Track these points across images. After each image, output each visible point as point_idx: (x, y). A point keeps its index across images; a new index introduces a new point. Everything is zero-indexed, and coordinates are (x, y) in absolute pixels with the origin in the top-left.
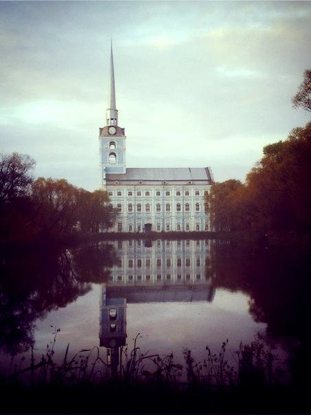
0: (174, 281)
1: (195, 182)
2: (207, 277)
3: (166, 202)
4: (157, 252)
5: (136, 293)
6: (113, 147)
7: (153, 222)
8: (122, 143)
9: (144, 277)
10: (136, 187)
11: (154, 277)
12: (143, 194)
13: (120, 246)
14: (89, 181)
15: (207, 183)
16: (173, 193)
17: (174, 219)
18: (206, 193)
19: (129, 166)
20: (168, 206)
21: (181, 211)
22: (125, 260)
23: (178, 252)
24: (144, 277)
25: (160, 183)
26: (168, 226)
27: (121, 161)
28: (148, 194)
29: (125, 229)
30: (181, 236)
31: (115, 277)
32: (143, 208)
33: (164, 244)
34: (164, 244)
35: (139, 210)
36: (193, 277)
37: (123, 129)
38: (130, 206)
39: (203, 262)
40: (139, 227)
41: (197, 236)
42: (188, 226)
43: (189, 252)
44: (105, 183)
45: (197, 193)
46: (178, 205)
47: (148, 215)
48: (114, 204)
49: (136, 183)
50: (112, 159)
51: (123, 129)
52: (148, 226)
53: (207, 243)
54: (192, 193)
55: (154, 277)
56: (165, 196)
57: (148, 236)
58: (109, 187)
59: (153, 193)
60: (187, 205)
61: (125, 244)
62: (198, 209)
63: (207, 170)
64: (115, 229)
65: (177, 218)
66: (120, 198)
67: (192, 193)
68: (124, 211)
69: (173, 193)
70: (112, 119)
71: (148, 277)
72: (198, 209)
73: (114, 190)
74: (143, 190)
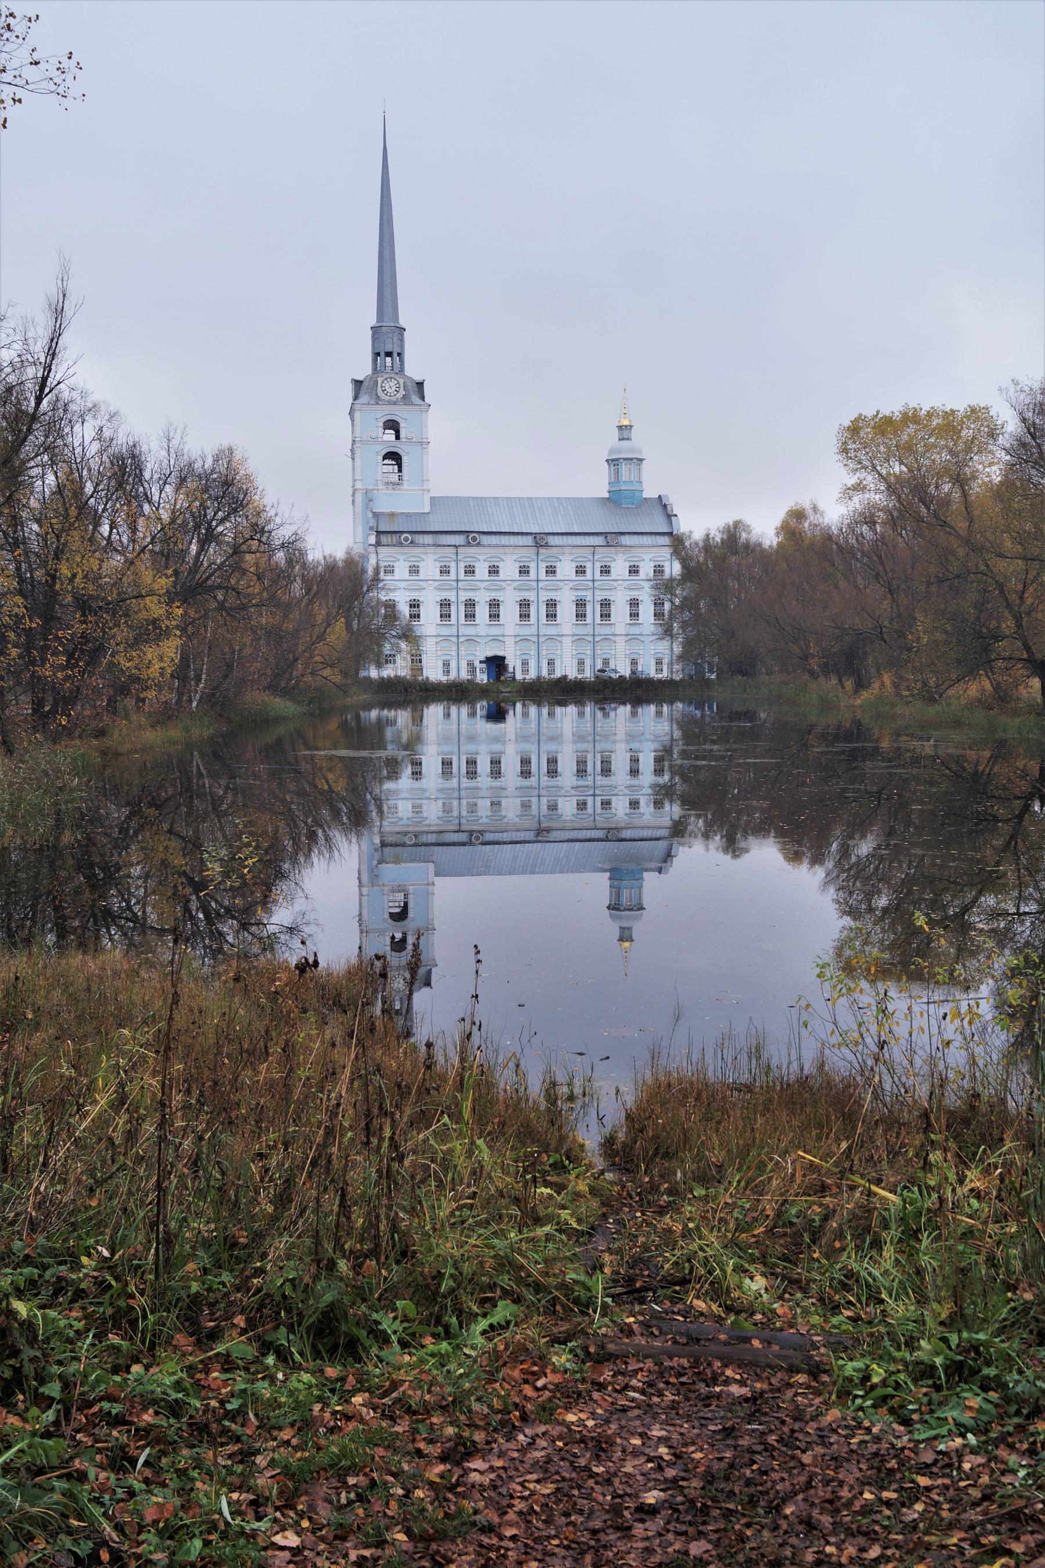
2: (658, 804)
4: (522, 738)
5: (464, 842)
6: (390, 436)
10: (460, 550)
12: (482, 571)
13: (418, 719)
14: (328, 536)
16: (566, 569)
17: (567, 642)
18: (659, 570)
19: (438, 490)
20: (552, 604)
21: (589, 619)
22: (431, 759)
23: (579, 738)
24: (484, 805)
25: (529, 540)
26: (551, 663)
28: (494, 571)
29: (433, 672)
31: (404, 809)
32: (482, 612)
33: (539, 714)
34: (539, 714)
35: (470, 616)
36: (620, 807)
37: (420, 385)
38: (445, 604)
39: (647, 763)
40: (471, 665)
41: (635, 691)
43: (556, 738)
44: (373, 540)
45: (634, 570)
47: (495, 631)
48: (402, 601)
52: (496, 664)
53: (659, 714)
54: (620, 568)
56: (462, 576)
57: (495, 691)
59: (509, 569)
61: (434, 712)
62: (634, 615)
64: (399, 668)
65: (579, 639)
67: (620, 568)
69: (566, 569)
70: (389, 354)
72: (634, 615)
73: (386, 554)
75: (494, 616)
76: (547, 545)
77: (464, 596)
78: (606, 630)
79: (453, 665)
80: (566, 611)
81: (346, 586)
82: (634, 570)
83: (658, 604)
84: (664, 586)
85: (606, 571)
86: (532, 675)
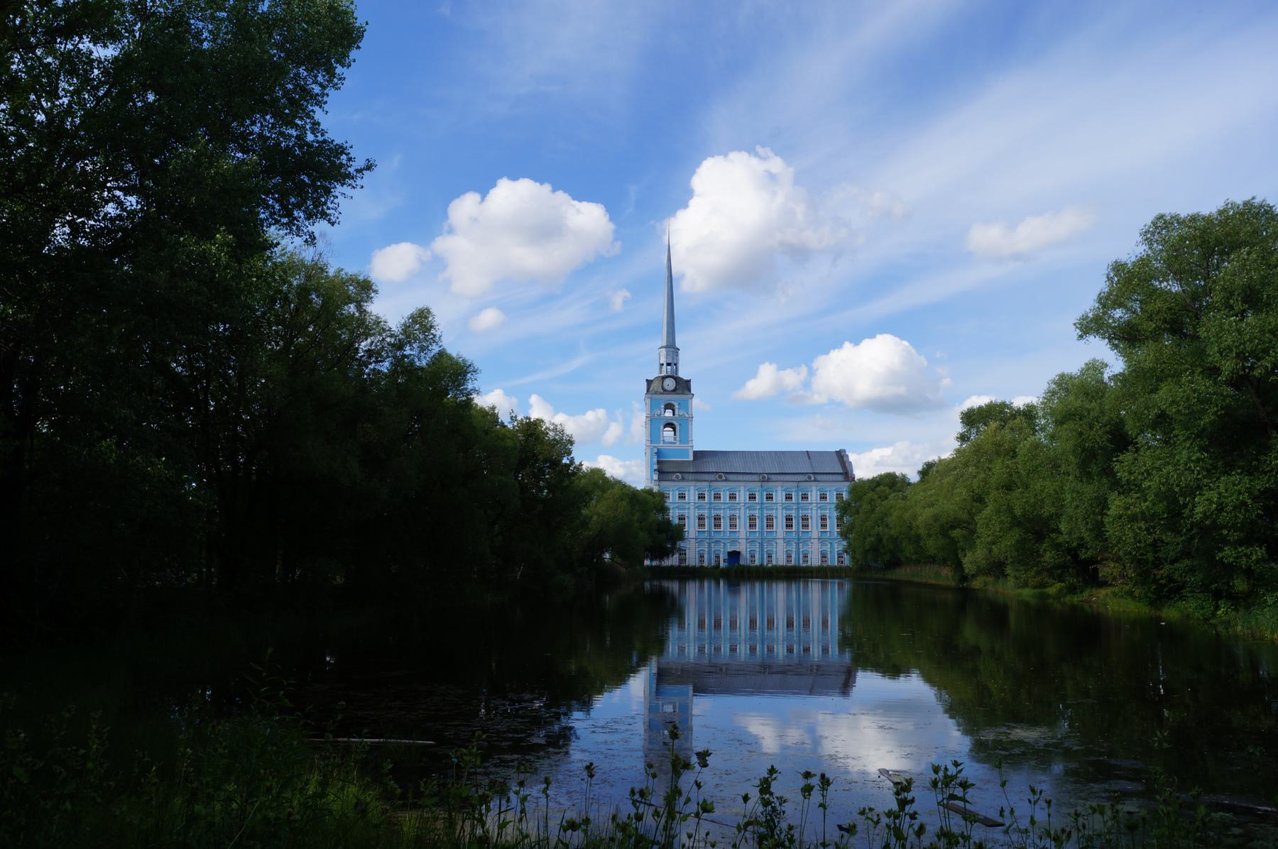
0: (781, 657)
1: (819, 477)
3: (766, 513)
6: (669, 413)
7: (742, 547)
8: (686, 406)
9: (725, 649)
10: (715, 484)
11: (743, 650)
12: (725, 497)
13: (682, 590)
15: (840, 478)
16: (779, 496)
17: (781, 542)
18: (839, 496)
19: (699, 446)
22: (691, 617)
24: (725, 649)
25: (756, 478)
26: (770, 556)
27: (686, 438)
28: (733, 497)
29: (692, 560)
30: (794, 574)
32: (725, 523)
36: (816, 651)
37: (689, 381)
38: (701, 518)
41: (824, 573)
42: (806, 556)
44: (656, 477)
45: (823, 497)
46: (789, 519)
47: (733, 536)
48: (673, 516)
49: (712, 477)
50: (668, 433)
51: (689, 381)
52: (734, 555)
54: (814, 496)
55: (743, 650)
57: (736, 573)
58: (664, 484)
59: (742, 496)
60: (805, 519)
61: (692, 589)
62: (824, 526)
63: (841, 456)
64: (673, 561)
65: (787, 542)
66: (685, 504)
67: (814, 496)
68: (691, 529)
69: (779, 496)
70: (669, 364)
71: (733, 649)
72: (824, 526)
74: (724, 489)
75: (733, 526)
76: (768, 481)
77: (714, 513)
78: (805, 536)
79: (706, 556)
80: (779, 524)
81: (645, 506)
82: (823, 497)
83: (840, 519)
84: (844, 508)
85: (805, 497)
86: (757, 563)
